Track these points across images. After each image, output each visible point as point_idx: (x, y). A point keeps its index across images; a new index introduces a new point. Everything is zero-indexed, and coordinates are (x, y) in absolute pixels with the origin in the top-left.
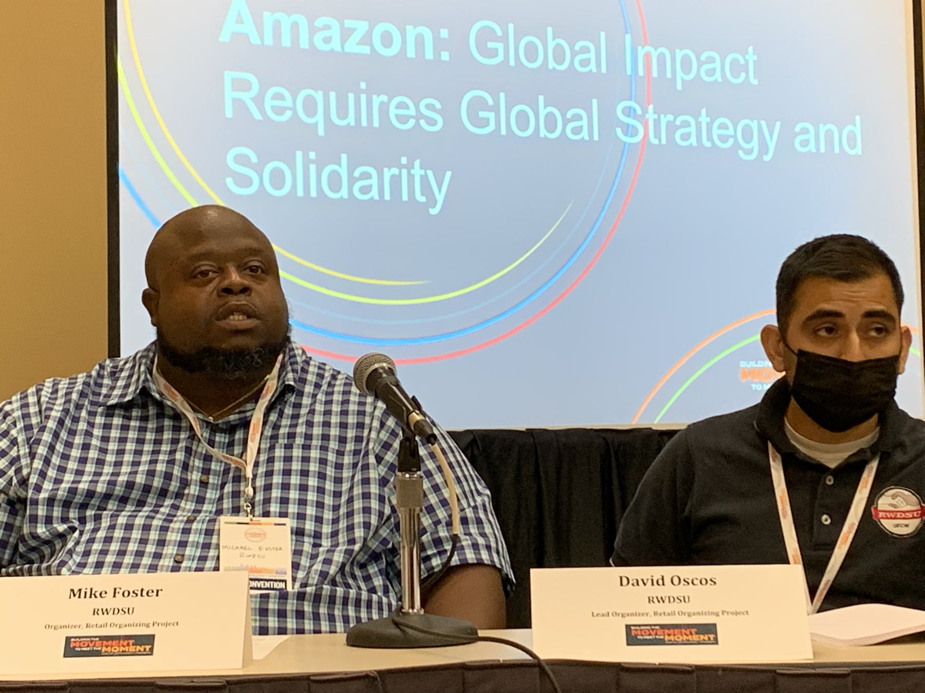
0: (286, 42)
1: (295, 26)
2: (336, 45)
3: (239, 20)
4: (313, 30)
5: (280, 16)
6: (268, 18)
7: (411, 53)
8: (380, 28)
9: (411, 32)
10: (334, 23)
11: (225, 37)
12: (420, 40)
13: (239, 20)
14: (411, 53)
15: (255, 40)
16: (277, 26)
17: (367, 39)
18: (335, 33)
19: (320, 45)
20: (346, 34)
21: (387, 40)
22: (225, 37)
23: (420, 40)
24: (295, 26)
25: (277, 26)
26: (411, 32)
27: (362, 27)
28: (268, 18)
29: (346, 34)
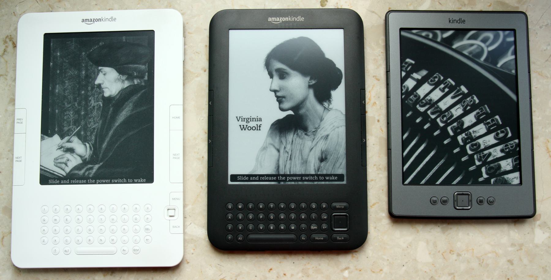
0: (274, 20)
2: (279, 20)
4: (276, 19)
7: (286, 20)
8: (283, 18)
9: (286, 18)
10: (278, 18)
12: (287, 19)
14: (286, 20)
16: (273, 19)
17: (282, 19)
19: (277, 20)
20: (280, 19)
21: (284, 19)
23: (287, 19)
25: (273, 19)
27: (281, 18)
29: (280, 19)
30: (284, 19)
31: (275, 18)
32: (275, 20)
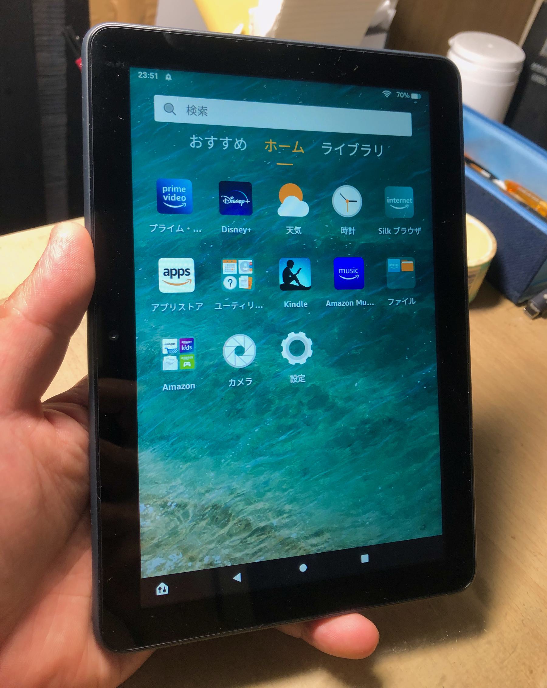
0: (334, 305)
1: (335, 303)
3: (328, 304)
4: (338, 303)
5: (334, 302)
6: (332, 303)
9: (350, 302)
10: (340, 302)
11: (327, 306)
12: (352, 303)
13: (328, 304)
14: (350, 305)
15: (330, 306)
17: (345, 304)
18: (341, 304)
20: (342, 303)
22: (327, 306)
23: (352, 303)
24: (335, 303)
25: (333, 303)
26: (350, 302)
27: (344, 302)
28: (332, 303)
30: (347, 303)
31: (336, 302)
32: (337, 305)
